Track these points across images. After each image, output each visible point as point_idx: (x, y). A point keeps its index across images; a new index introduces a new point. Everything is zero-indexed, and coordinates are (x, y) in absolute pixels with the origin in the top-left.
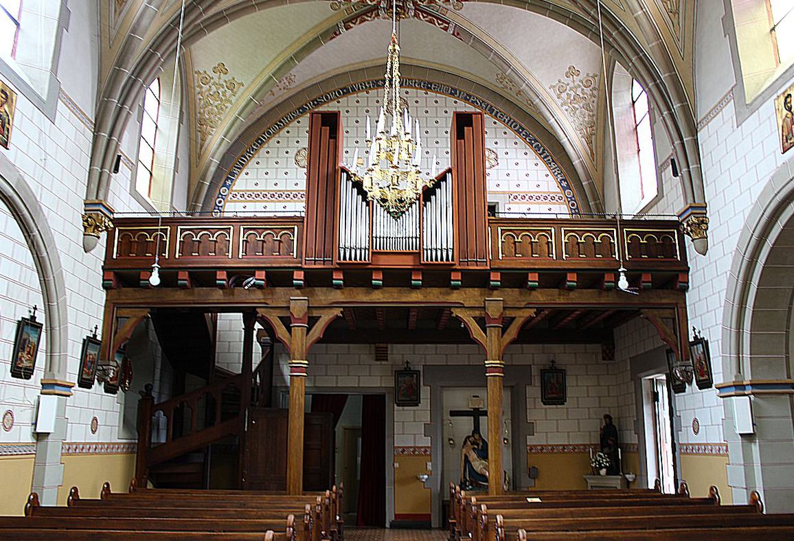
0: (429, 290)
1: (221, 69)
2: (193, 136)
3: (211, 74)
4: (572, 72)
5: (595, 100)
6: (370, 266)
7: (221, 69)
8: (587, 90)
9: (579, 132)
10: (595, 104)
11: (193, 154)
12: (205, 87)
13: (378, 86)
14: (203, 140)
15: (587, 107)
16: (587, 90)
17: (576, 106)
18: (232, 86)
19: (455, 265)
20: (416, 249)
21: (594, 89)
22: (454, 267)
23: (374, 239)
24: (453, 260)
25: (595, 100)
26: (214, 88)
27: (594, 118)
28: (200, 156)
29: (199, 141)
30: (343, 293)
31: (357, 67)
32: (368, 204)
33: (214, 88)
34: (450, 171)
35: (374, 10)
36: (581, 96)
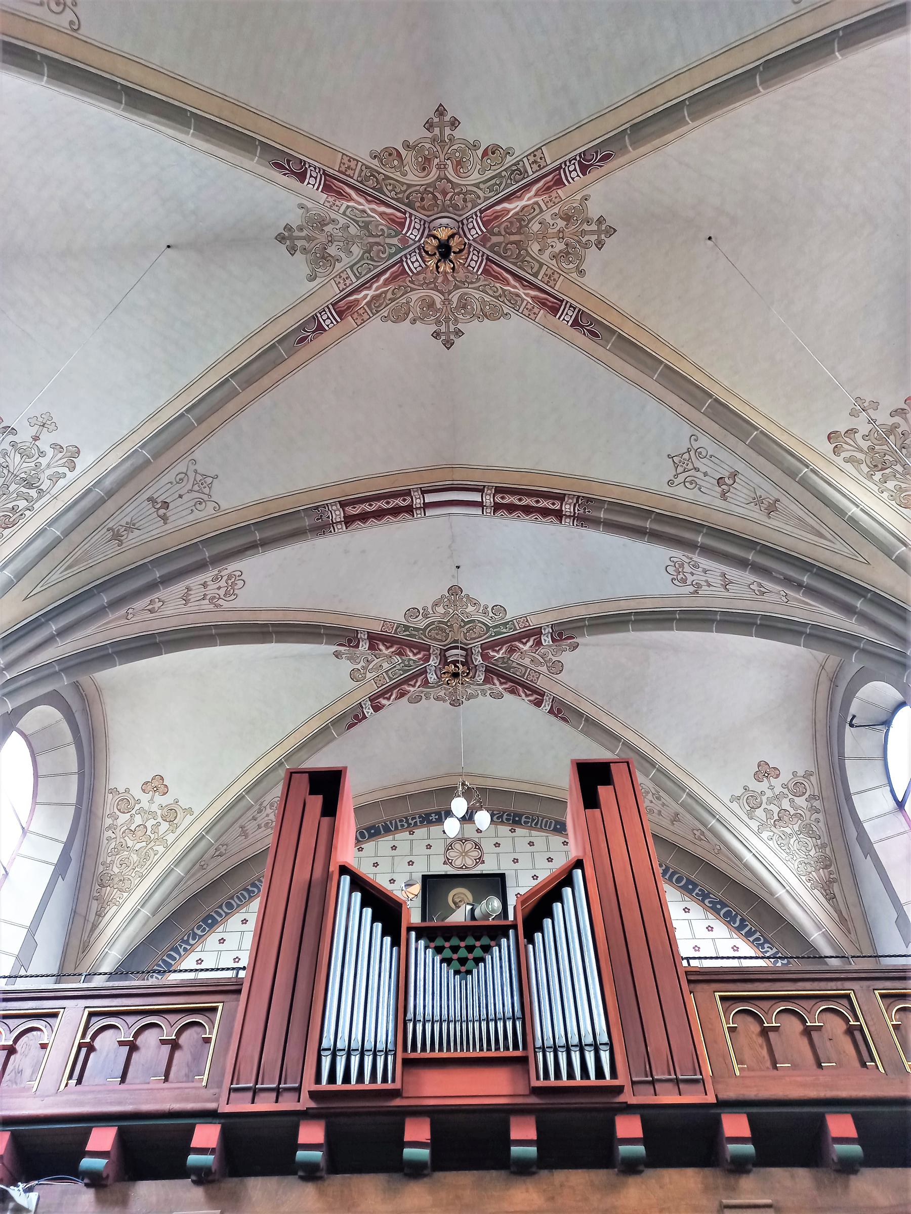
0: (560, 1176)
1: (157, 785)
2: (82, 910)
3: (137, 793)
4: (765, 771)
5: (820, 816)
6: (397, 1102)
7: (157, 785)
8: (801, 801)
9: (804, 878)
10: (821, 824)
11: (75, 942)
12: (123, 818)
13: (430, 822)
14: (100, 915)
15: (808, 830)
16: (801, 801)
17: (788, 830)
18: (171, 814)
19: (619, 1090)
20: (516, 1047)
21: (813, 797)
22: (621, 1099)
23: (410, 1026)
24: (614, 1074)
25: (820, 816)
26: (138, 820)
27: (828, 849)
28: (85, 947)
29: (92, 917)
30: (322, 1193)
31: (394, 793)
32: (396, 943)
33: (138, 820)
34: (579, 864)
35: (421, 674)
36: (792, 812)
